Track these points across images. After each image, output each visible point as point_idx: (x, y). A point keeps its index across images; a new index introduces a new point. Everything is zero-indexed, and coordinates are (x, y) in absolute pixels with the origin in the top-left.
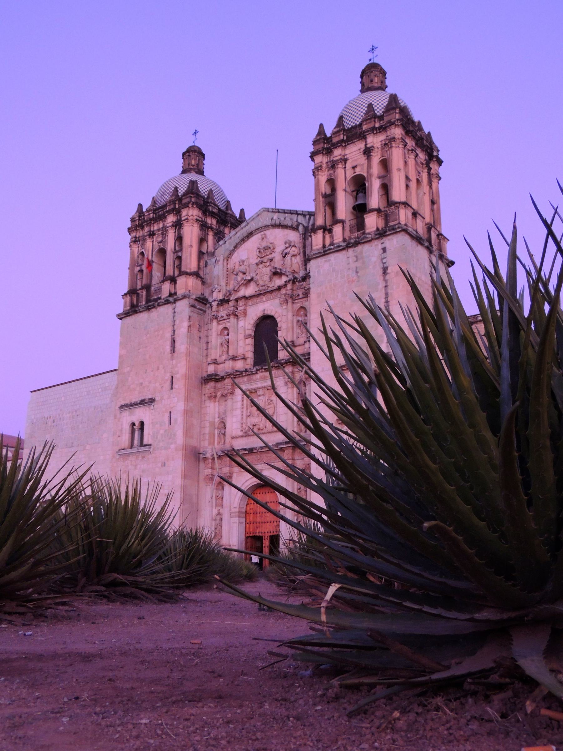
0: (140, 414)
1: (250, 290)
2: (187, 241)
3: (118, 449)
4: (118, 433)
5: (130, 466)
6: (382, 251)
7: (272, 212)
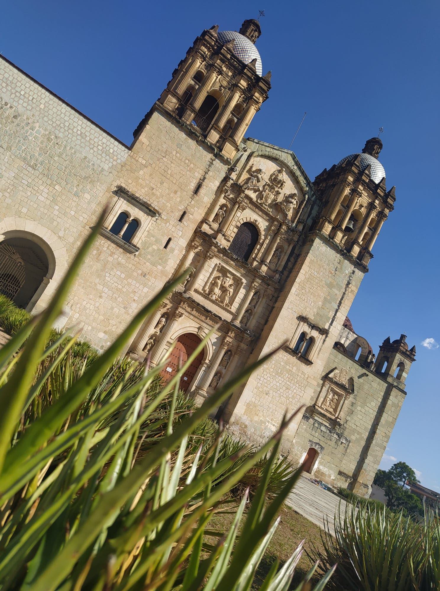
5: (105, 249)
6: (352, 272)
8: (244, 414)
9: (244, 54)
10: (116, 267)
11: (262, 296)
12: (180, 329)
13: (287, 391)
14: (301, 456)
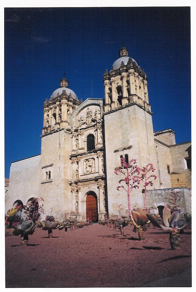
0: (48, 169)
1: (84, 126)
2: (62, 111)
4: (42, 176)
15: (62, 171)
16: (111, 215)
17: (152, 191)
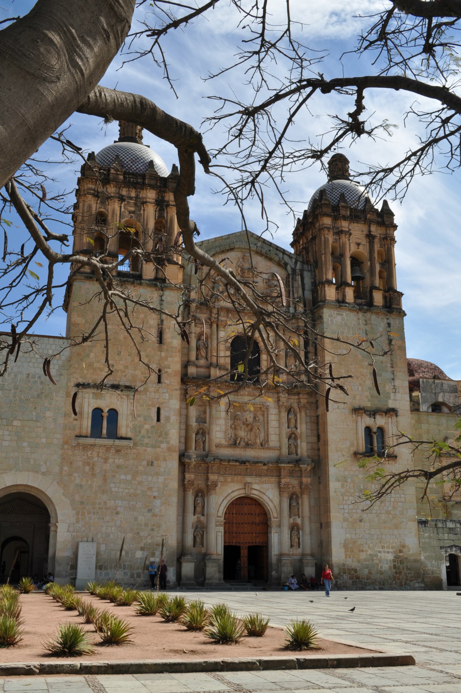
3: (75, 435)
5: (96, 459)
6: (387, 326)
7: (256, 239)
8: (346, 558)
9: (136, 165)
10: (117, 472)
11: (297, 410)
12: (223, 500)
13: (383, 504)
14: (440, 571)
15: (171, 421)
16: (340, 569)
17: (437, 523)
